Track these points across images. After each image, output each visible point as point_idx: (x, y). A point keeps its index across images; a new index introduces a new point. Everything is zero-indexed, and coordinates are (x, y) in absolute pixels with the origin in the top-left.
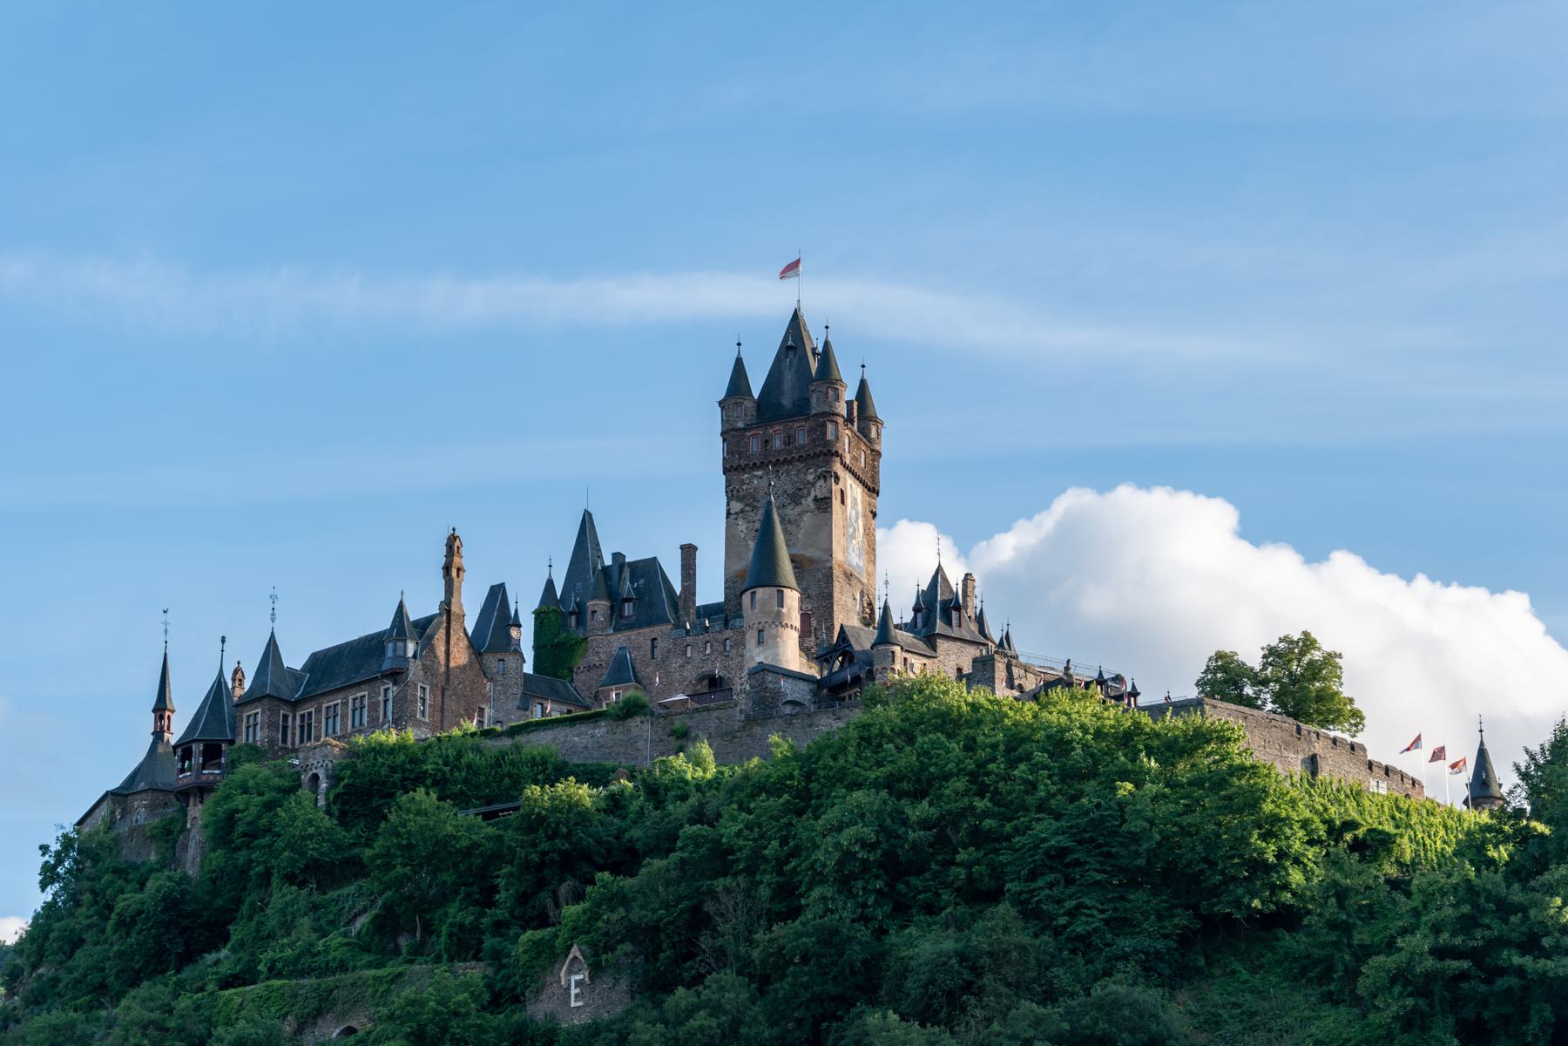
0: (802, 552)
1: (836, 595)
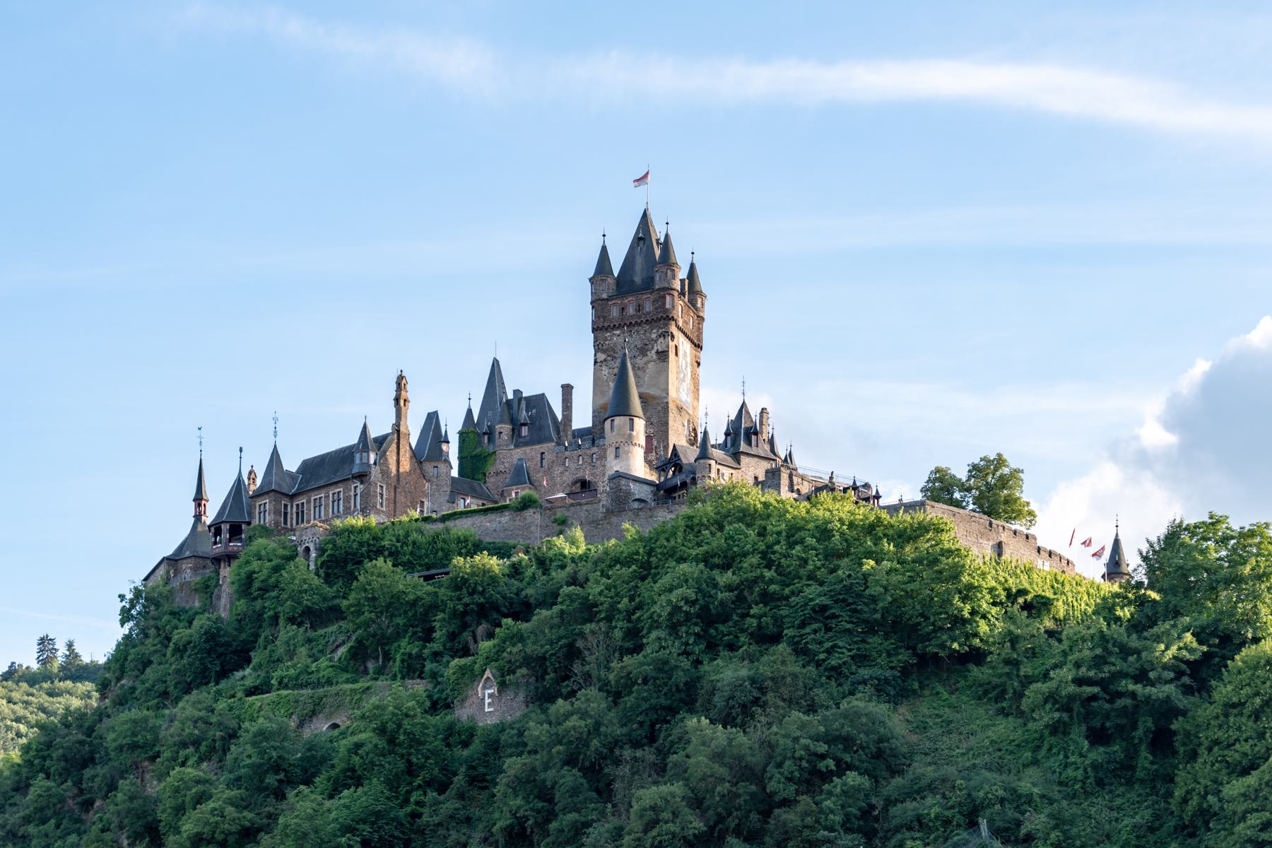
0: (647, 391)
1: (671, 423)
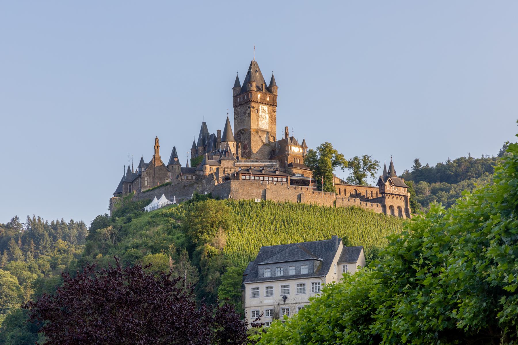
0: (246, 128)
1: (251, 138)
